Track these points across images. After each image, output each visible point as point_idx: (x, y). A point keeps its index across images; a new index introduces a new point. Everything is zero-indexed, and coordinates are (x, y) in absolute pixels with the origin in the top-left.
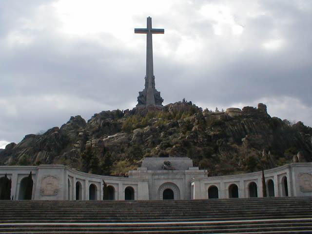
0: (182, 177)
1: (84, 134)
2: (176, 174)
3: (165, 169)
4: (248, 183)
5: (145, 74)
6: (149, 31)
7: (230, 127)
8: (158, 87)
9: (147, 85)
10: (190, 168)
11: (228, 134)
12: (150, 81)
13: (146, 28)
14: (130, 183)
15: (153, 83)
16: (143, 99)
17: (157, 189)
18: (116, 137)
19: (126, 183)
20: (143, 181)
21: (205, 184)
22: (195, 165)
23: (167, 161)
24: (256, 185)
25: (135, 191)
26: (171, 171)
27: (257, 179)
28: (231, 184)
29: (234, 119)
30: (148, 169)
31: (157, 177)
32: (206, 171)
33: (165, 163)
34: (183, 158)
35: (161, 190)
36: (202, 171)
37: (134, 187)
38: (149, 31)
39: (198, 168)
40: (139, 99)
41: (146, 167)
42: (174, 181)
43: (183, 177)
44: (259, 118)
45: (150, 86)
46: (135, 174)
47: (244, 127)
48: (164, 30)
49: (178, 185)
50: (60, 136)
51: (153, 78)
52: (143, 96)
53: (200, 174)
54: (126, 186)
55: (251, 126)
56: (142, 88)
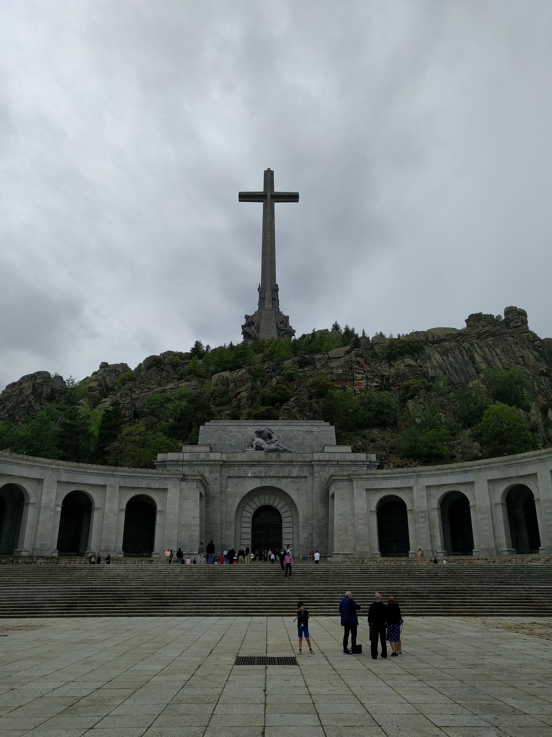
0: (306, 474)
1: (100, 385)
2: (290, 463)
3: (259, 448)
4: (502, 488)
5: (257, 280)
6: (269, 196)
7: (437, 356)
8: (285, 308)
9: (262, 299)
10: (327, 449)
11: (432, 373)
12: (268, 294)
13: (262, 190)
14: (144, 484)
15: (275, 300)
16: (253, 329)
17: (236, 505)
18: (171, 389)
19: (129, 483)
20: (184, 479)
21: (367, 490)
22: (340, 441)
24: (531, 495)
25: (159, 508)
26: (274, 456)
27: (535, 474)
28: (446, 490)
29: (444, 340)
30: (211, 451)
31: (234, 471)
32: (373, 457)
33: (259, 434)
34: (310, 423)
35: (248, 508)
36: (362, 456)
37: (156, 497)
38: (269, 196)
39: (348, 449)
40: (248, 330)
41: (206, 445)
42: (282, 485)
43: (305, 472)
44: (510, 338)
45: (268, 305)
46: (176, 463)
47: (472, 358)
48: (298, 193)
49: (294, 497)
50: (46, 391)
51: (275, 289)
52: (253, 323)
53: (354, 463)
54: (132, 494)
55: (490, 357)
56: (252, 308)
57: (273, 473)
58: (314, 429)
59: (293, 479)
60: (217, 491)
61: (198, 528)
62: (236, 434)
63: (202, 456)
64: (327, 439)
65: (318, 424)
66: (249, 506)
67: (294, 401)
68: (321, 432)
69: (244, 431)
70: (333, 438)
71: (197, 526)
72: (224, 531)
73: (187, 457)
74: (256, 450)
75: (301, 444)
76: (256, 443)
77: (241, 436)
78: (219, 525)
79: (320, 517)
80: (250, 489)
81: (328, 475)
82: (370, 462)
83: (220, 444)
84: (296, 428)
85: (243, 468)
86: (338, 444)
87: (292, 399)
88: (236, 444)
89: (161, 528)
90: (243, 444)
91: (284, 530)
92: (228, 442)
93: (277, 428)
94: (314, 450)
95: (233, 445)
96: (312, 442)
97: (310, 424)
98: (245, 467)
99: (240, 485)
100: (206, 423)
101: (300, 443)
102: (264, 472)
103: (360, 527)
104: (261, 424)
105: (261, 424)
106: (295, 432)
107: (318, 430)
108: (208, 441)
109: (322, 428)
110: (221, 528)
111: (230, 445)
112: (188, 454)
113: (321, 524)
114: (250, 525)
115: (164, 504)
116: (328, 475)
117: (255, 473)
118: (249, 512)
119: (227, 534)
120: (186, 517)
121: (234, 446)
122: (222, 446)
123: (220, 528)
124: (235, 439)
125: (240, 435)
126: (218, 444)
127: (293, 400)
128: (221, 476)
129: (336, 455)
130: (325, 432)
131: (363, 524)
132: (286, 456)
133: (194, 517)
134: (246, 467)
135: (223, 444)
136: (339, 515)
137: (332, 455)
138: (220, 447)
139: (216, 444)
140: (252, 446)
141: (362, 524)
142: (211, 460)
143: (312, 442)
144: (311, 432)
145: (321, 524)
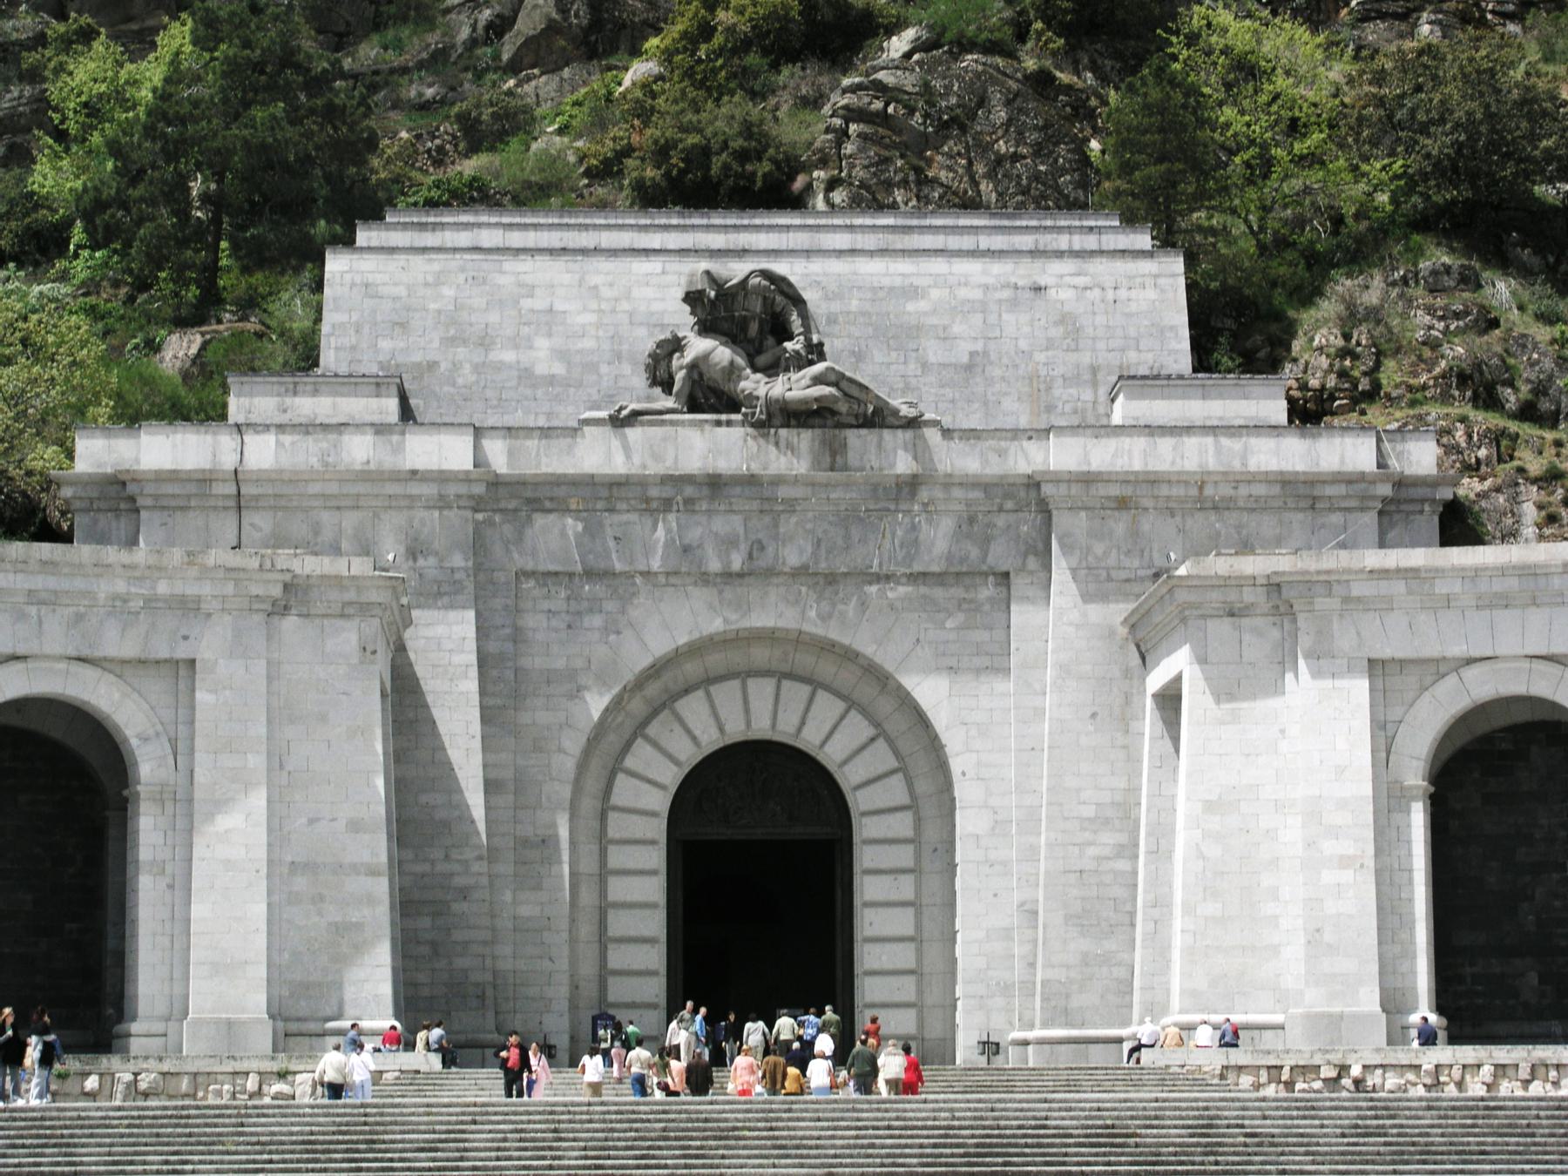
23: (736, 270)
25: (149, 767)
57: (801, 551)
58: (1052, 272)
59: (923, 590)
60: (458, 659)
61: (381, 887)
62: (559, 306)
63: (359, 450)
64: (1132, 332)
65: (1079, 242)
66: (648, 748)
67: (908, 55)
68: (1097, 292)
69: (611, 285)
70: (1172, 328)
71: (372, 872)
72: (508, 896)
73: (262, 453)
74: (694, 406)
75: (969, 368)
76: (693, 366)
77: (591, 318)
78: (480, 858)
79: (1089, 811)
80: (659, 644)
81: (1136, 563)
82: (1401, 483)
83: (456, 366)
84: (938, 266)
85: (616, 518)
86: (1195, 370)
87: (898, 45)
88: (559, 369)
89: (171, 887)
90: (604, 369)
91: (867, 888)
92: (509, 356)
93: (817, 266)
94: (1050, 408)
95: (541, 369)
96: (1040, 357)
97: (1025, 241)
98: (625, 517)
99: (597, 621)
100: (363, 236)
101: (965, 359)
102: (744, 547)
103: (1329, 877)
104: (717, 240)
105: (717, 240)
106: (935, 294)
107: (1081, 281)
108: (385, 344)
109: (1101, 268)
110: (492, 877)
111: (526, 375)
112: (270, 439)
113: (1092, 851)
114: (656, 858)
115: (181, 748)
116: (1136, 563)
117: (686, 549)
118: (649, 781)
119: (525, 911)
120: (312, 821)
121: (551, 380)
122: (474, 378)
123: (484, 881)
124: (550, 335)
125: (585, 309)
126: (443, 366)
127: (905, 48)
128: (478, 568)
129: (1192, 443)
130: (1123, 294)
131: (1344, 862)
132: (879, 445)
133: (355, 826)
134: (633, 517)
135: (478, 368)
136: (1210, 807)
137: (1165, 444)
138: (460, 381)
139: (432, 366)
140: (667, 386)
141: (1342, 857)
142: (414, 472)
143: (1040, 357)
144: (1038, 289)
145: (1092, 851)
